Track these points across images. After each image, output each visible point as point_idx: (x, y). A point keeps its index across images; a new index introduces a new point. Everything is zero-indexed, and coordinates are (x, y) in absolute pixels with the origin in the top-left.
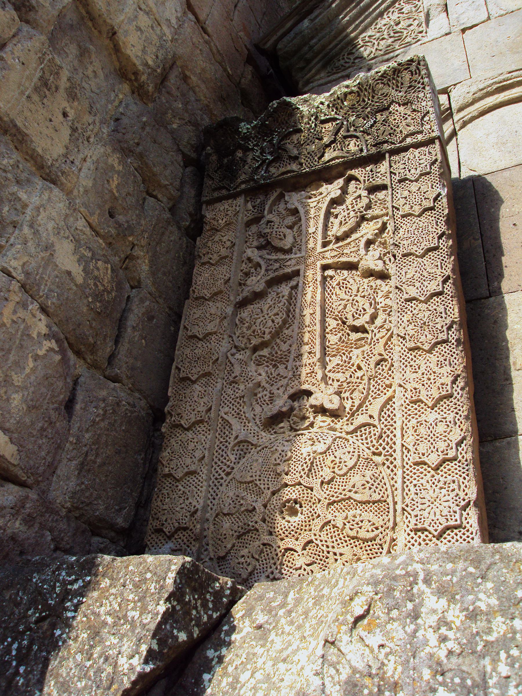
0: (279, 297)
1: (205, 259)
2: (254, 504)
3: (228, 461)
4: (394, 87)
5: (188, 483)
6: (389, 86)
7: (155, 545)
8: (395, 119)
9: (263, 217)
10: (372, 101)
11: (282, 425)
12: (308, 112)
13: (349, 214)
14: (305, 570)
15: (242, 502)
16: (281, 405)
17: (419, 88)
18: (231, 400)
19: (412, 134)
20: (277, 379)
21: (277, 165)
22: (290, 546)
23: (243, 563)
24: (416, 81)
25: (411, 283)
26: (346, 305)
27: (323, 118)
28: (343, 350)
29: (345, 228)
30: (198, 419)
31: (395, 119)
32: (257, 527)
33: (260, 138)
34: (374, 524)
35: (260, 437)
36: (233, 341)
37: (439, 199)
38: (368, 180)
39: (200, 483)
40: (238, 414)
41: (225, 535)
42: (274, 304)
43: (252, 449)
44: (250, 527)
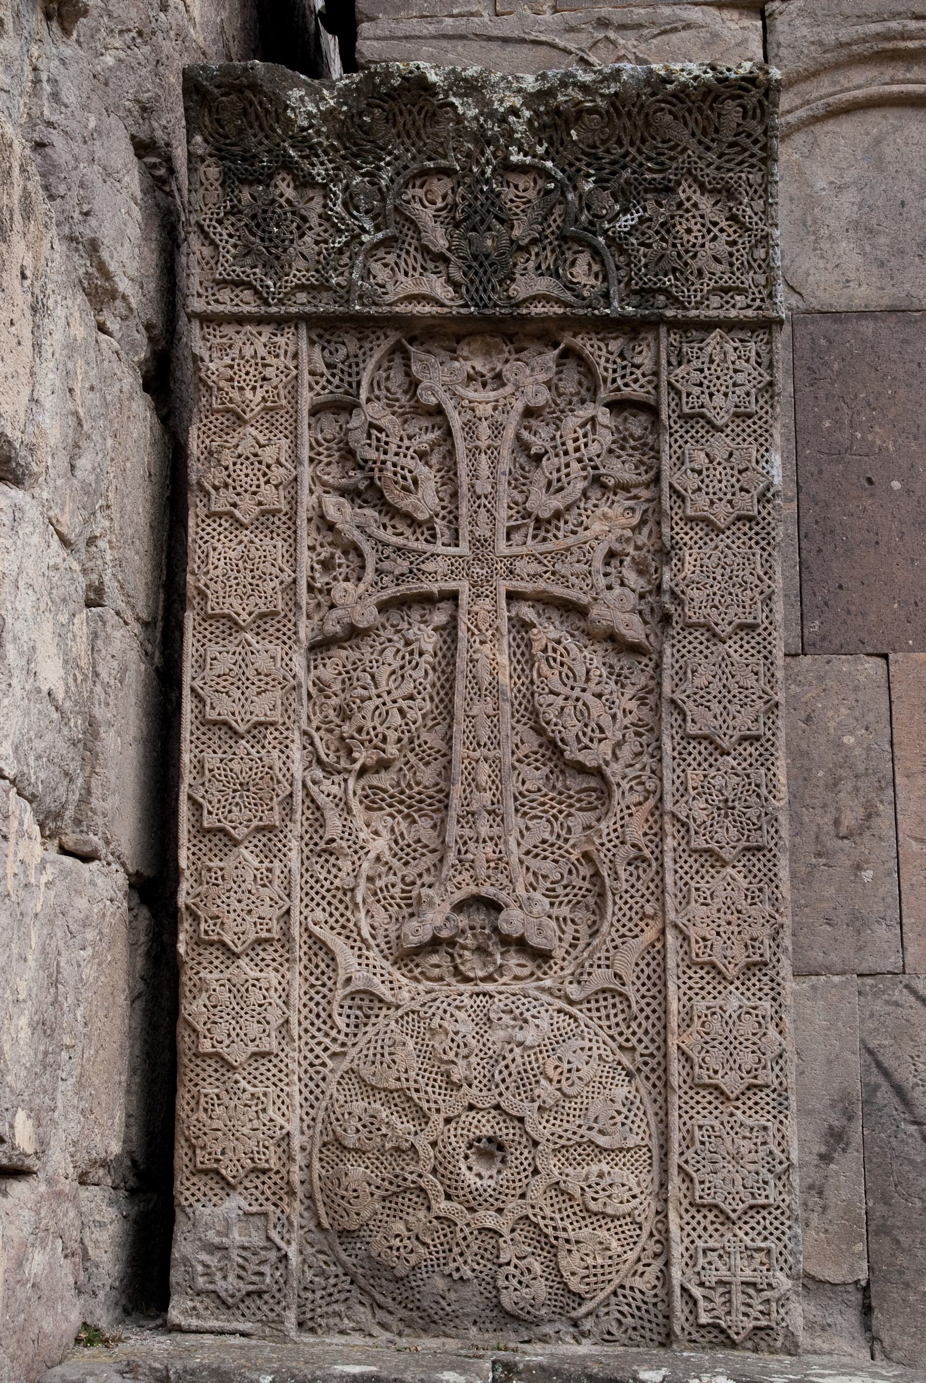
0: (411, 653)
2: (411, 1138)
3: (332, 1028)
5: (257, 1073)
6: (686, 125)
9: (357, 406)
10: (640, 152)
11: (435, 959)
12: (474, 125)
13: (567, 465)
14: (516, 1267)
15: (384, 1130)
16: (439, 922)
17: (753, 155)
18: (323, 891)
19: (726, 290)
20: (415, 851)
21: (391, 259)
22: (488, 1225)
24: (749, 136)
25: (703, 701)
26: (562, 708)
28: (553, 807)
29: (557, 502)
30: (264, 935)
33: (344, 157)
36: (312, 744)
37: (769, 495)
39: (282, 1076)
40: (344, 927)
42: (402, 667)
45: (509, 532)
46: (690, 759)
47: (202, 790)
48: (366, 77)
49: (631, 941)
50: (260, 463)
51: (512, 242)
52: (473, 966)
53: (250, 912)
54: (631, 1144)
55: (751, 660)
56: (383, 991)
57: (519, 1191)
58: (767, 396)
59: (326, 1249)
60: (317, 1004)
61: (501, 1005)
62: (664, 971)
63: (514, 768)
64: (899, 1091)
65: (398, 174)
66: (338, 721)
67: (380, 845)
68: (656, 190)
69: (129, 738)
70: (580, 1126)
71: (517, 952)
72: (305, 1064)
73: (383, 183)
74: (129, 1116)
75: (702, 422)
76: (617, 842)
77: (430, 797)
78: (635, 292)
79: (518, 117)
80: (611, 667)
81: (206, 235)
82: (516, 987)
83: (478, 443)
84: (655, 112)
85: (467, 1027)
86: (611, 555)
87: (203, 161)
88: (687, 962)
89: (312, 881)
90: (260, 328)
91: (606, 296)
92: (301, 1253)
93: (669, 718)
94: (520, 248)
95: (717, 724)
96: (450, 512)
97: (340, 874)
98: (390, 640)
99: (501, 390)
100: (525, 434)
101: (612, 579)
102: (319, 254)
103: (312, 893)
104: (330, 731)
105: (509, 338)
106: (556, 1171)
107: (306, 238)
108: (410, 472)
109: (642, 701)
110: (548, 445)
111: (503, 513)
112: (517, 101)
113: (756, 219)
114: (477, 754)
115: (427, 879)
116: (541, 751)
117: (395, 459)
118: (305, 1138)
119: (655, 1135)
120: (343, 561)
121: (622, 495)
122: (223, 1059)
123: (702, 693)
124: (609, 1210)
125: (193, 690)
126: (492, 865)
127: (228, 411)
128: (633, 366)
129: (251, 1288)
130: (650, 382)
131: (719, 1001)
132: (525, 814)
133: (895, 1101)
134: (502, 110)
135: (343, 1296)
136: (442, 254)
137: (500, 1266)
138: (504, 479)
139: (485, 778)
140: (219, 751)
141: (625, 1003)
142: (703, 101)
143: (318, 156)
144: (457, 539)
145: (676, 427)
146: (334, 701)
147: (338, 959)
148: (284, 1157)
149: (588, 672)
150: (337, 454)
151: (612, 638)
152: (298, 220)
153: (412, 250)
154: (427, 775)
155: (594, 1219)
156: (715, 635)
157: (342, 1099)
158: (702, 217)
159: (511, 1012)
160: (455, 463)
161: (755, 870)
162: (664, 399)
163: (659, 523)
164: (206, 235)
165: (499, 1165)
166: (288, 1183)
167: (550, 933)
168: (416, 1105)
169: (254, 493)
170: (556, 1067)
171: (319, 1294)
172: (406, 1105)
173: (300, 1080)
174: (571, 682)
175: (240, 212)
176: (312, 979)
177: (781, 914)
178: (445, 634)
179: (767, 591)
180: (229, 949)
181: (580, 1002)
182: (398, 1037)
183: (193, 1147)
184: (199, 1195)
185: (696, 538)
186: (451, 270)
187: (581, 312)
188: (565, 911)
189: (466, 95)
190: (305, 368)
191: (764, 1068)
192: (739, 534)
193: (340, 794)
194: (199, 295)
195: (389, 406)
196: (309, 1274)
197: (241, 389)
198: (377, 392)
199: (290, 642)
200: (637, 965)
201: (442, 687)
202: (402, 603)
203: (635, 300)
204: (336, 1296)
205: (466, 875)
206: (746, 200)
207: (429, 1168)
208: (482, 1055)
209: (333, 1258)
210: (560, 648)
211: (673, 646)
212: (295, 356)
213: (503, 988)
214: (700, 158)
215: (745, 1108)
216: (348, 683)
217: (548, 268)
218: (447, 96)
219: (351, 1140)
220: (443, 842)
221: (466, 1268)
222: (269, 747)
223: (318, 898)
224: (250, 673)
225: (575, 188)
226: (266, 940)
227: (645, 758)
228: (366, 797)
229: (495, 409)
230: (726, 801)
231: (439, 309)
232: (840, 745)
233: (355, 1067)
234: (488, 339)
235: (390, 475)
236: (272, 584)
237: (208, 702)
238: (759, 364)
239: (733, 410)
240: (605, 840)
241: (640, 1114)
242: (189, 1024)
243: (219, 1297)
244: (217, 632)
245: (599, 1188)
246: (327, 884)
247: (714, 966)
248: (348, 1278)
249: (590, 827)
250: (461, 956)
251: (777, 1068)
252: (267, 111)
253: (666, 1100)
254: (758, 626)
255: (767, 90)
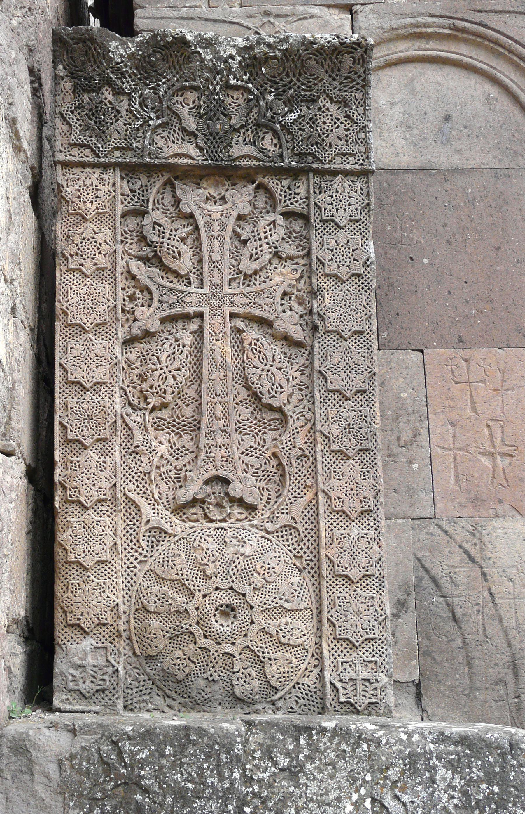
0: (179, 346)
1: (74, 263)
2: (185, 605)
3: (139, 547)
4: (329, 71)
5: (99, 572)
6: (323, 66)
7: (71, 640)
8: (324, 123)
9: (147, 212)
10: (298, 80)
11: (194, 510)
12: (211, 64)
13: (261, 246)
14: (242, 673)
15: (170, 601)
16: (196, 490)
17: (358, 84)
19: (344, 155)
20: (182, 452)
21: (165, 134)
22: (228, 651)
23: (179, 665)
24: (356, 73)
26: (260, 376)
27: (232, 82)
28: (256, 429)
29: (256, 266)
30: (102, 497)
31: (324, 123)
32: (192, 630)
33: (140, 79)
34: (302, 631)
35: (173, 524)
36: (126, 394)
37: (368, 263)
38: (285, 201)
39: (113, 573)
40: (144, 493)
41: (155, 634)
42: (174, 353)
43: (165, 537)
44: (184, 630)
45: (231, 280)
46: (329, 403)
47: (67, 419)
48: (152, 36)
49: (300, 499)
50: (96, 242)
51: (231, 126)
52: (215, 514)
53: (94, 485)
54: (302, 607)
55: (361, 350)
56: (167, 527)
57: (244, 633)
58: (366, 211)
59: (138, 666)
60: (131, 535)
61: (231, 534)
62: (317, 515)
63: (235, 408)
64: (434, 580)
65: (169, 89)
66: (139, 382)
67: (163, 449)
68: (307, 101)
69: (27, 390)
70: (275, 598)
71: (238, 506)
72: (125, 567)
73: (161, 93)
74: (27, 597)
75: (333, 224)
76: (291, 447)
77: (190, 423)
78: (296, 155)
79: (234, 60)
80: (285, 354)
81: (65, 119)
82: (239, 524)
83: (213, 233)
84: (307, 60)
85: (213, 546)
86: (285, 294)
87: (63, 79)
88: (330, 510)
89: (127, 468)
90: (94, 170)
91: (281, 156)
92: (125, 668)
93: (318, 381)
94: (235, 130)
95: (343, 383)
96: (198, 270)
97: (142, 465)
98: (166, 339)
99: (225, 205)
100: (238, 229)
101: (285, 307)
102: (126, 131)
103: (127, 474)
104: (135, 388)
105: (228, 178)
106: (263, 622)
107: (119, 122)
108: (177, 248)
109: (302, 372)
110: (250, 235)
111: (228, 271)
112: (233, 52)
113: (359, 117)
114: (215, 400)
115: (188, 467)
116: (249, 398)
117: (169, 241)
118: (126, 607)
119: (314, 602)
120: (140, 296)
121: (289, 262)
122: (81, 564)
123: (335, 367)
124: (291, 642)
125: (61, 365)
126: (225, 459)
127: (77, 214)
128: (295, 193)
129: (99, 687)
130: (304, 202)
131: (347, 531)
132: (241, 432)
133: (432, 585)
134: (225, 56)
135: (148, 691)
136: (193, 132)
137: (234, 673)
138: (227, 253)
139: (220, 412)
140: (76, 398)
141: (297, 533)
142: (332, 54)
143: (126, 78)
144: (202, 284)
145: (319, 226)
146: (136, 371)
147: (142, 510)
148: (115, 617)
149: (274, 356)
150: (136, 239)
151: (286, 338)
152: (115, 112)
153: (176, 129)
154: (188, 412)
155: (283, 647)
156: (341, 337)
157: (146, 585)
158: (331, 115)
159: (237, 537)
160: (200, 244)
161: (365, 461)
162: (312, 211)
163: (310, 278)
164: (65, 119)
165: (232, 619)
166: (118, 631)
167: (257, 496)
168: (187, 588)
169: (93, 259)
170: (262, 567)
171: (135, 690)
172: (182, 588)
173: (122, 575)
174: (264, 362)
175: (83, 107)
176: (128, 521)
177: (379, 485)
178: (196, 335)
179: (369, 314)
180: (83, 505)
181: (273, 533)
182: (176, 552)
183: (65, 612)
184: (69, 638)
185: (330, 285)
186: (199, 140)
187: (268, 164)
188: (263, 484)
189: (206, 47)
190: (119, 191)
191: (372, 566)
192: (353, 283)
193: (141, 421)
194: (61, 152)
195: (163, 213)
196: (129, 680)
197: (85, 202)
198: (157, 205)
199: (113, 339)
200: (303, 512)
201: (195, 364)
202: (173, 319)
203: (297, 158)
204: (144, 692)
205: (211, 465)
206: (354, 107)
207: (195, 621)
208: (222, 561)
209: (142, 671)
210: (258, 343)
211: (319, 342)
212: (114, 185)
213: (231, 525)
214: (330, 85)
215: (362, 587)
216: (144, 362)
217: (250, 141)
218: (196, 48)
219: (152, 607)
220: (198, 447)
221: (216, 674)
222: (103, 396)
223: (130, 477)
224: (92, 355)
225: (264, 99)
226: (103, 500)
227: (305, 402)
228: (155, 423)
229: (222, 215)
230: (349, 425)
231: (192, 162)
232: (399, 398)
233: (152, 568)
234: (217, 178)
235: (166, 250)
236: (103, 308)
237: (69, 371)
238: (362, 194)
239: (349, 218)
240: (284, 446)
241: (306, 591)
242: (62, 545)
243: (81, 693)
244: (73, 333)
245: (286, 630)
246: (135, 470)
247: (344, 512)
248: (151, 682)
249: (276, 439)
250: (208, 508)
251: (378, 566)
252: (98, 53)
253: (319, 584)
254: (364, 332)
255: (366, 50)
